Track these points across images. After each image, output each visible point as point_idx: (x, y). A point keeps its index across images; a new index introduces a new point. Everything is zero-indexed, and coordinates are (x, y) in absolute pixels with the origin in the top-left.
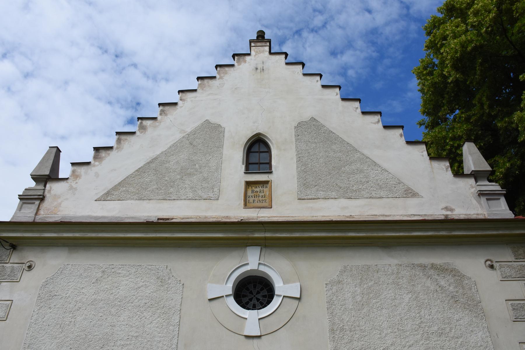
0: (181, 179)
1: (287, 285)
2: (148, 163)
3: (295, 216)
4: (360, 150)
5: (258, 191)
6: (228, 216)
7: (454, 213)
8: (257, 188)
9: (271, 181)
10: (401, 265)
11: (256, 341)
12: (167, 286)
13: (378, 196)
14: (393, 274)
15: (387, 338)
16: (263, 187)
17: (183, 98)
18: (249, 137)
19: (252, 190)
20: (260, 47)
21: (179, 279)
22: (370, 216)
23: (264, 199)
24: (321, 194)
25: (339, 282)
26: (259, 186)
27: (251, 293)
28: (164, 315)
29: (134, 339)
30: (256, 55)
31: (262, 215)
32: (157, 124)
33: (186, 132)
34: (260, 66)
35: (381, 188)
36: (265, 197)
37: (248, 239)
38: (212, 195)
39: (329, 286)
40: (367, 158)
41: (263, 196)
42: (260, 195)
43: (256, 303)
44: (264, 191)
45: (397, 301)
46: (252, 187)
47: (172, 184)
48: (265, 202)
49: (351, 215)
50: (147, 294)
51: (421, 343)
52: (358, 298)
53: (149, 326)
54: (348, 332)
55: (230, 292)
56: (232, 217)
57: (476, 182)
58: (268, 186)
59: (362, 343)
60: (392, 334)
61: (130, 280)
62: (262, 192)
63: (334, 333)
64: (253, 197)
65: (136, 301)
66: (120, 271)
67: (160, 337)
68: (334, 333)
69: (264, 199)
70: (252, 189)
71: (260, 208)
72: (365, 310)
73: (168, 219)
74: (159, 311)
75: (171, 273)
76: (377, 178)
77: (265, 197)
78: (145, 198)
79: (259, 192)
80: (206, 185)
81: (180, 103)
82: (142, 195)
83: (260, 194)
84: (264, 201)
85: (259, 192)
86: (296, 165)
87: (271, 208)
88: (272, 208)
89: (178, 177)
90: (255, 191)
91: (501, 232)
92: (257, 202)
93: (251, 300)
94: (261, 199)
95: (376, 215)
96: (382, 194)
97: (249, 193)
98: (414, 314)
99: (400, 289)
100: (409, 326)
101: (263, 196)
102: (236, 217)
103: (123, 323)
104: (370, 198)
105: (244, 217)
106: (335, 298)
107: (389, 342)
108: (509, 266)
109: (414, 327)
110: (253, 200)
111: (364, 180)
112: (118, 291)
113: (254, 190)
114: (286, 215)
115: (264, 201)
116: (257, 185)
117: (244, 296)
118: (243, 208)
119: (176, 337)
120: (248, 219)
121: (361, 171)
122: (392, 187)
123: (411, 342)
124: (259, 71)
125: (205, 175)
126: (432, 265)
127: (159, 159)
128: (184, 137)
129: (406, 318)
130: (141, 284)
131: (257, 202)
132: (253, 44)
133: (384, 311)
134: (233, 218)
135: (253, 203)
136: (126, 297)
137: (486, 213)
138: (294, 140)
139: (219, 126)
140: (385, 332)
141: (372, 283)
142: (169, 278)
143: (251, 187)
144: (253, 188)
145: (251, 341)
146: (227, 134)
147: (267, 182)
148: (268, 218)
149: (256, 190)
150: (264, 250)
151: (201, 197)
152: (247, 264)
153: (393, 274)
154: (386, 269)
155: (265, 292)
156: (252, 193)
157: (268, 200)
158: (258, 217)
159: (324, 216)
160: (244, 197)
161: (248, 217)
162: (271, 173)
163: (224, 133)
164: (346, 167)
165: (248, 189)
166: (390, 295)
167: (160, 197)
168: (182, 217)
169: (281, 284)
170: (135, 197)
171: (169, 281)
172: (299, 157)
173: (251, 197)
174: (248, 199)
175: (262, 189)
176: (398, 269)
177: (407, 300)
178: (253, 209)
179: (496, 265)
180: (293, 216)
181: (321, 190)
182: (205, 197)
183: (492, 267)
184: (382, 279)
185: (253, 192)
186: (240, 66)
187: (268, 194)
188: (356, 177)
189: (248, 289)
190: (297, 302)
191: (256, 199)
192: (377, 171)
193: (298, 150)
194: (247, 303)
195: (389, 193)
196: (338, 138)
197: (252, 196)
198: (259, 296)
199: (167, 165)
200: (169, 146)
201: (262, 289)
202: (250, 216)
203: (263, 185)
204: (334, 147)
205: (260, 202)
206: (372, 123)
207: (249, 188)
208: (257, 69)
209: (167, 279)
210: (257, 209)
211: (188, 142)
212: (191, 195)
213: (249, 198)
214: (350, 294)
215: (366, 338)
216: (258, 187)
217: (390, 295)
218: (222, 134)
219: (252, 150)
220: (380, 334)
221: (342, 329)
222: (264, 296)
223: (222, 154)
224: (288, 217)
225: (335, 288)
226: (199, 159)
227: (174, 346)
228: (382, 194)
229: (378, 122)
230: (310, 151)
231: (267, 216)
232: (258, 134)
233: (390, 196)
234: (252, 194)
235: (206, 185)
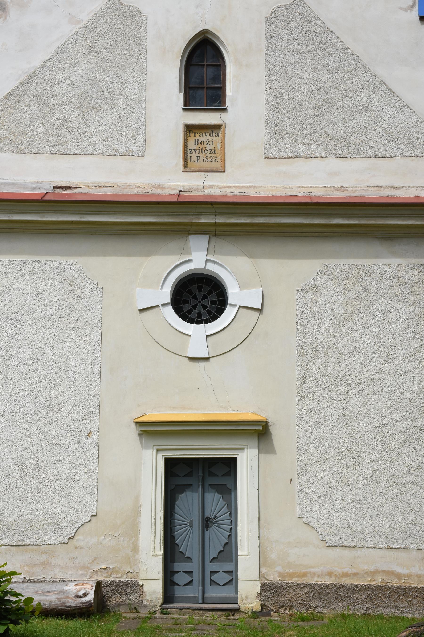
0: (82, 116)
1: (244, 291)
2: (23, 84)
3: (259, 185)
4: (371, 68)
5: (205, 141)
6: (159, 185)
8: (202, 136)
9: (224, 125)
10: (404, 266)
11: (202, 364)
12: (79, 291)
13: (389, 154)
14: (391, 278)
15: (372, 364)
16: (211, 134)
18: (188, 38)
19: (195, 140)
21: (95, 281)
22: (371, 189)
23: (213, 155)
24: (301, 150)
25: (316, 288)
26: (205, 133)
27: (195, 297)
28: (79, 331)
29: (41, 362)
31: (211, 184)
33: (79, 22)
35: (395, 139)
36: (215, 153)
37: (192, 224)
38: (133, 149)
39: (301, 294)
40: (382, 83)
41: (212, 150)
42: (208, 149)
43: (203, 311)
44: (214, 142)
45: (392, 317)
46: (195, 133)
47: (68, 125)
48: (215, 161)
49: (342, 187)
50: (52, 303)
51: (416, 371)
52: (340, 311)
53: (60, 345)
54: (322, 355)
55: (169, 300)
56: (166, 187)
58: (219, 134)
59: (339, 369)
60: (380, 359)
61: (25, 282)
62: (211, 143)
63: (303, 356)
64: (197, 152)
65: (38, 312)
66: (7, 270)
67: (77, 360)
68: (303, 356)
69: (213, 155)
70: (195, 138)
71: (208, 172)
72: (347, 327)
73: (69, 188)
74: (71, 326)
75: (83, 272)
76: (391, 121)
77: (215, 152)
78: (28, 150)
79: (205, 144)
80: (124, 129)
82: (22, 144)
83: (207, 146)
84: (214, 159)
85: (205, 144)
86: (265, 95)
87: (224, 172)
88: (226, 172)
89: (77, 113)
90: (199, 142)
92: (203, 161)
93: (195, 307)
94: (208, 155)
95: (381, 187)
97: (191, 145)
98: (413, 334)
99: (399, 300)
100: (404, 349)
101: (212, 150)
102: (172, 187)
103: (22, 342)
104: (376, 156)
105: (183, 187)
106: (308, 309)
107: (375, 369)
109: (410, 351)
110: (198, 157)
111: (370, 125)
112: (9, 298)
113: (198, 140)
114: (245, 185)
115: (214, 159)
116: (203, 131)
117: (186, 302)
118: (183, 172)
119: (98, 359)
120: (189, 190)
121: (369, 109)
122: (414, 138)
123: (404, 371)
125: (121, 111)
127: (39, 76)
128: (77, 33)
129: (401, 338)
130: (42, 288)
131: (203, 161)
133: (372, 329)
134: (168, 188)
135: (197, 161)
136: (22, 307)
138: (264, 46)
140: (371, 356)
141: (361, 290)
142: (81, 280)
143: (193, 134)
145: (196, 364)
146: (151, 31)
148: (220, 188)
149: (201, 139)
150: (213, 239)
151: (116, 150)
152: (190, 261)
153: (391, 278)
154: (383, 270)
155: (214, 297)
156: (195, 144)
157: (219, 158)
158: (204, 187)
159: (303, 187)
160: (183, 152)
161: (191, 187)
162: (225, 110)
163: (147, 27)
164: (345, 101)
165: (189, 138)
166: (383, 308)
167: (52, 149)
168: (91, 185)
169: (237, 290)
170: (11, 147)
171: (82, 284)
172: (271, 81)
173: (193, 151)
174: (189, 155)
175: (210, 138)
176: (400, 272)
177: (406, 315)
178: (197, 173)
180: (256, 185)
181: (302, 143)
182: (123, 150)
184: (375, 286)
185: (197, 143)
187: (219, 148)
188: (359, 119)
189: (190, 292)
190: (257, 314)
191: (202, 155)
192: (394, 109)
193: (269, 66)
194: (190, 312)
195: (406, 149)
196: (337, 42)
197: (195, 150)
198: (206, 302)
199: (55, 89)
200: (53, 51)
201: (210, 293)
202: (193, 185)
203: (213, 131)
204: (328, 61)
205: (207, 157)
206: (401, 8)
207: (190, 136)
209: (79, 282)
210: (203, 173)
211: (85, 44)
212: (101, 148)
213: (190, 153)
214: (329, 304)
215: (345, 363)
216: (204, 134)
217: (383, 308)
218: (142, 30)
219: (193, 62)
220: (364, 359)
221: (314, 351)
222: (213, 302)
223: (144, 70)
224: (250, 187)
226: (109, 79)
227: (96, 371)
228: (396, 149)
230: (289, 68)
231: (218, 186)
232: (204, 32)
233: (407, 154)
234: (196, 147)
235: (124, 129)
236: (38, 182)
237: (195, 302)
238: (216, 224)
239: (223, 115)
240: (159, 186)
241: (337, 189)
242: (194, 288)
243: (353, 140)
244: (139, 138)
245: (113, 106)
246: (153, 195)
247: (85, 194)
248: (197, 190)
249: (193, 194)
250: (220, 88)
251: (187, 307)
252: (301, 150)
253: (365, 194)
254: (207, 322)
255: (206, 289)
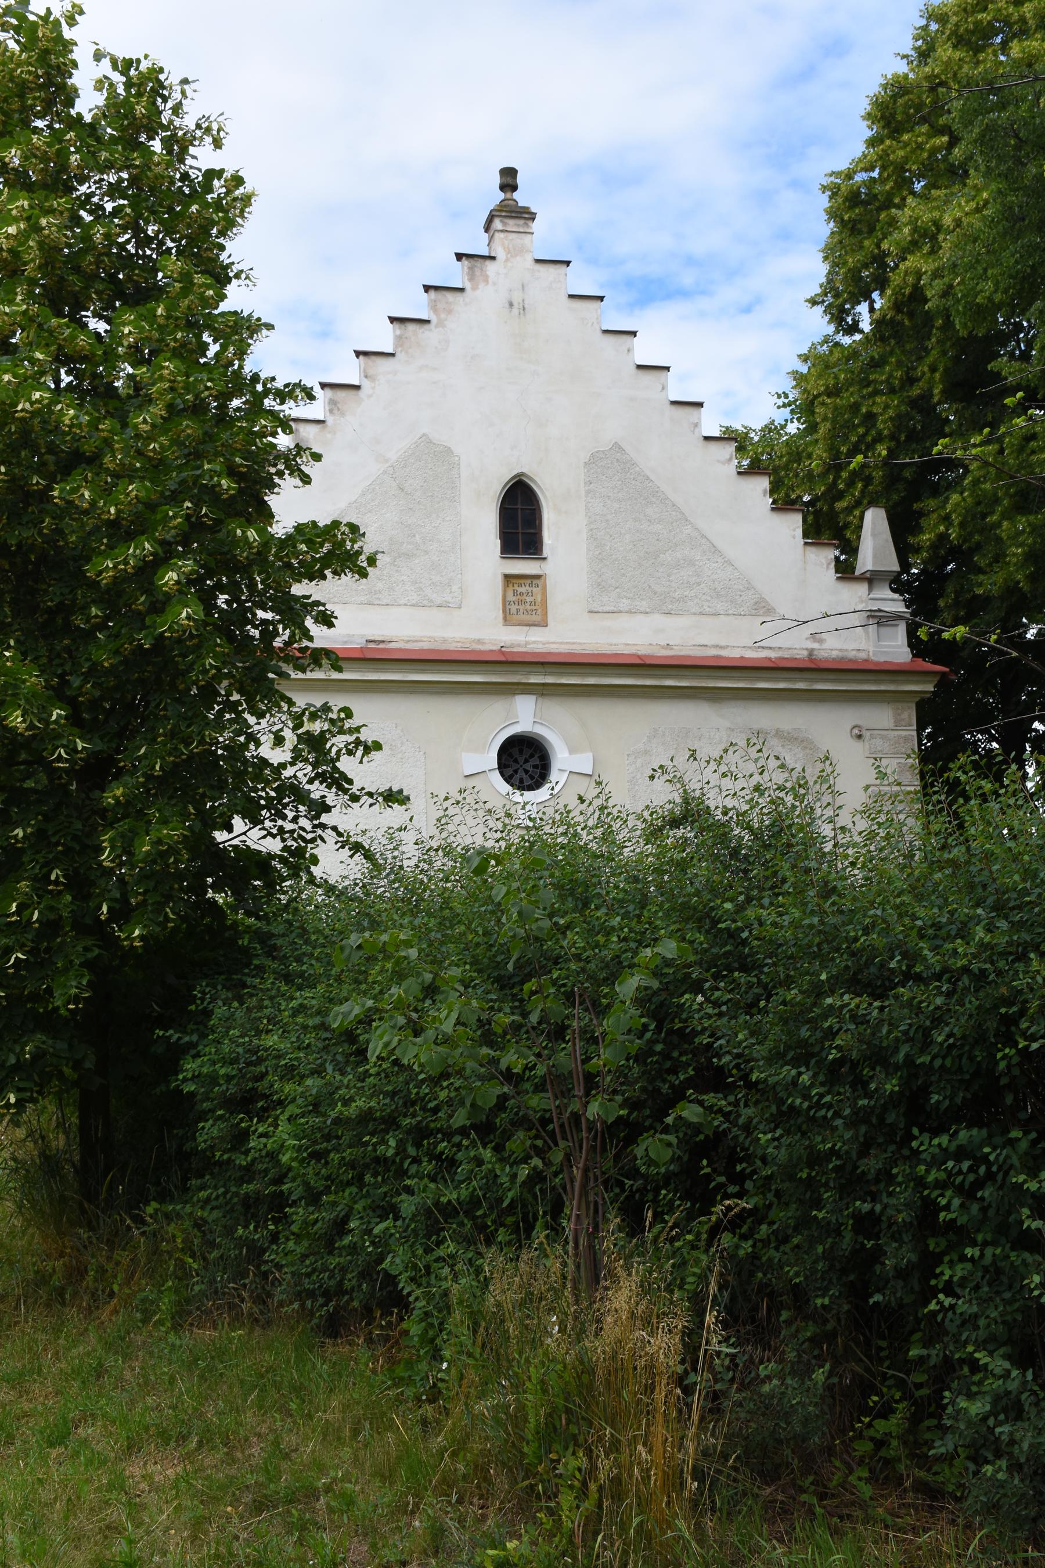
7: (825, 646)
17: (371, 372)
20: (514, 235)
25: (646, 752)
27: (516, 761)
30: (507, 260)
32: (329, 436)
33: (387, 461)
34: (517, 299)
40: (703, 536)
57: (870, 590)
81: (366, 385)
91: (883, 688)
93: (516, 771)
94: (528, 607)
96: (720, 607)
104: (701, 614)
108: (883, 737)
124: (515, 311)
126: (777, 731)
128: (384, 472)
132: (497, 224)
137: (871, 649)
139: (448, 451)
144: (516, 587)
147: (535, 578)
149: (520, 590)
150: (540, 699)
151: (431, 601)
155: (535, 761)
158: (527, 643)
167: (363, 599)
169: (566, 754)
179: (867, 734)
183: (860, 737)
186: (478, 293)
191: (521, 607)
198: (528, 766)
201: (532, 756)
208: (511, 305)
212: (414, 598)
222: (535, 767)
225: (639, 761)
228: (720, 607)
229: (730, 460)
232: (523, 474)
236: (348, 635)
237: (515, 766)
238: (544, 684)
239: (543, 564)
240: (479, 641)
241: (663, 647)
242: (515, 751)
243: (676, 595)
244: (455, 588)
245: (426, 552)
246: (473, 652)
247: (400, 650)
248: (519, 645)
249: (515, 650)
250: (535, 534)
251: (509, 772)
252: (624, 604)
253: (691, 653)
254: (530, 788)
255: (527, 752)
